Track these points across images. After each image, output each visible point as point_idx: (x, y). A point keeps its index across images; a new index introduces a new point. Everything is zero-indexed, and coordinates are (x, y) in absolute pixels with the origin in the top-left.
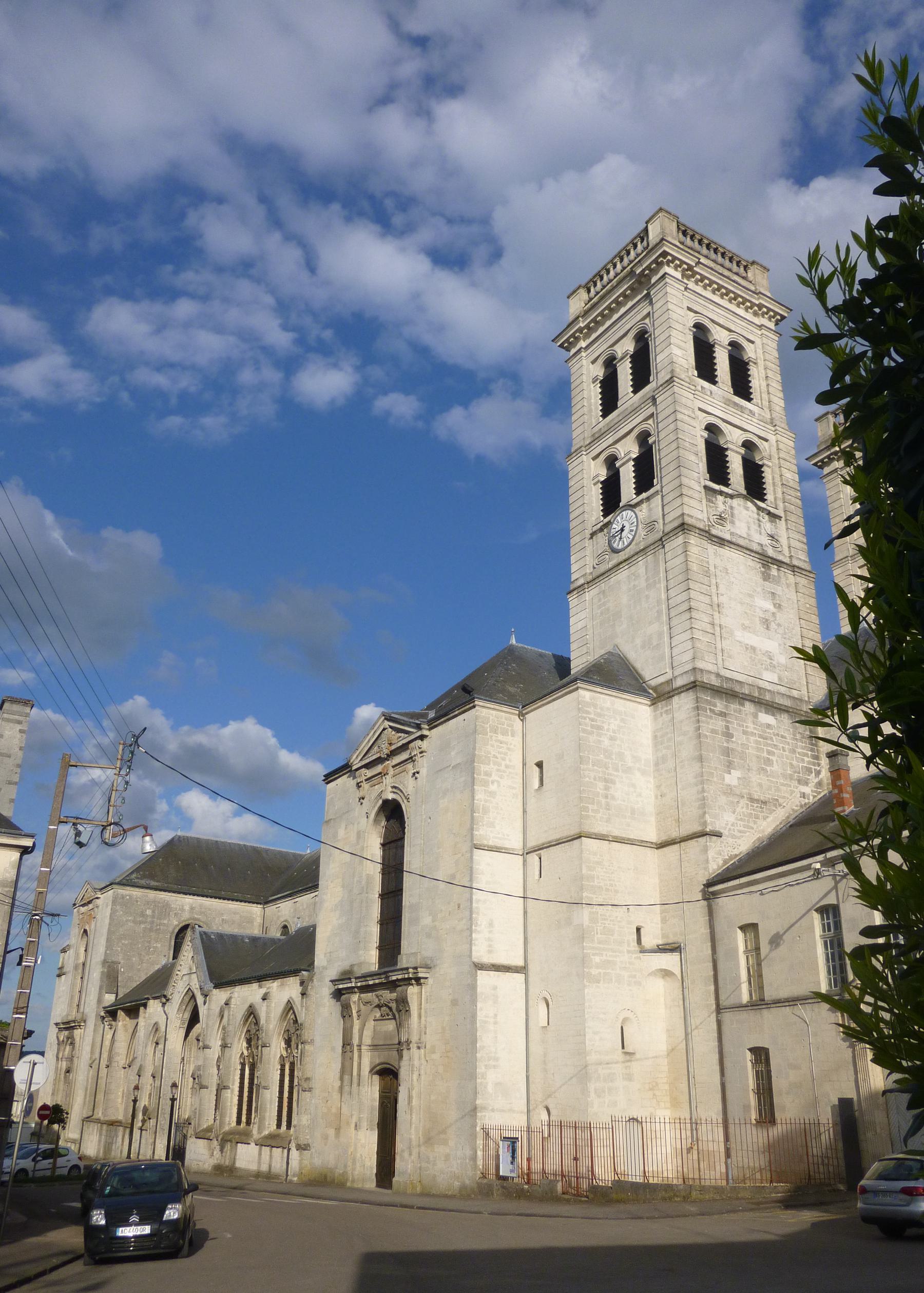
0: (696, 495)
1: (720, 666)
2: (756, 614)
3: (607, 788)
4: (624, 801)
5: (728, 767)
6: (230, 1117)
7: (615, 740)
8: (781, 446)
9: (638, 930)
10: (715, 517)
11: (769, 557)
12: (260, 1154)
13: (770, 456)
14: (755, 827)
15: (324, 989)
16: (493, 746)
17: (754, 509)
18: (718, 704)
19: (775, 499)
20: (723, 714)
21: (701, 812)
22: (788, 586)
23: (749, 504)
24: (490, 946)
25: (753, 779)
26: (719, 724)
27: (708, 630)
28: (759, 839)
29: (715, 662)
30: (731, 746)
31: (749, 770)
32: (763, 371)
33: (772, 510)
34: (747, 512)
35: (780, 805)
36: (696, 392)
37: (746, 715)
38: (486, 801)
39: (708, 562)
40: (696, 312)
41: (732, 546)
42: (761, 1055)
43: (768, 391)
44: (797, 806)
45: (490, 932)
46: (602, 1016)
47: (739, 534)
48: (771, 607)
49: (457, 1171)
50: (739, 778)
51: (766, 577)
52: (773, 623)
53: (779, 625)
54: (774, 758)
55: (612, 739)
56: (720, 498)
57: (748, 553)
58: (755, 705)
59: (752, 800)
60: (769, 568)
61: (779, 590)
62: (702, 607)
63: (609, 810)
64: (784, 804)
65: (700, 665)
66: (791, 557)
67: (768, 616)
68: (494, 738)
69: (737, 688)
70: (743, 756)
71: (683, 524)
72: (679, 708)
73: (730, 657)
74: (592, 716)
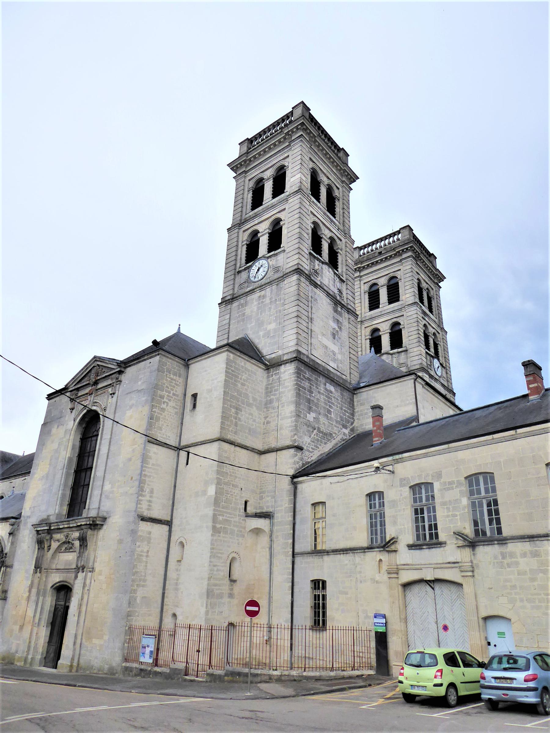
3: (237, 413)
4: (245, 423)
9: (246, 503)
16: (166, 380)
68: (168, 376)
74: (233, 369)
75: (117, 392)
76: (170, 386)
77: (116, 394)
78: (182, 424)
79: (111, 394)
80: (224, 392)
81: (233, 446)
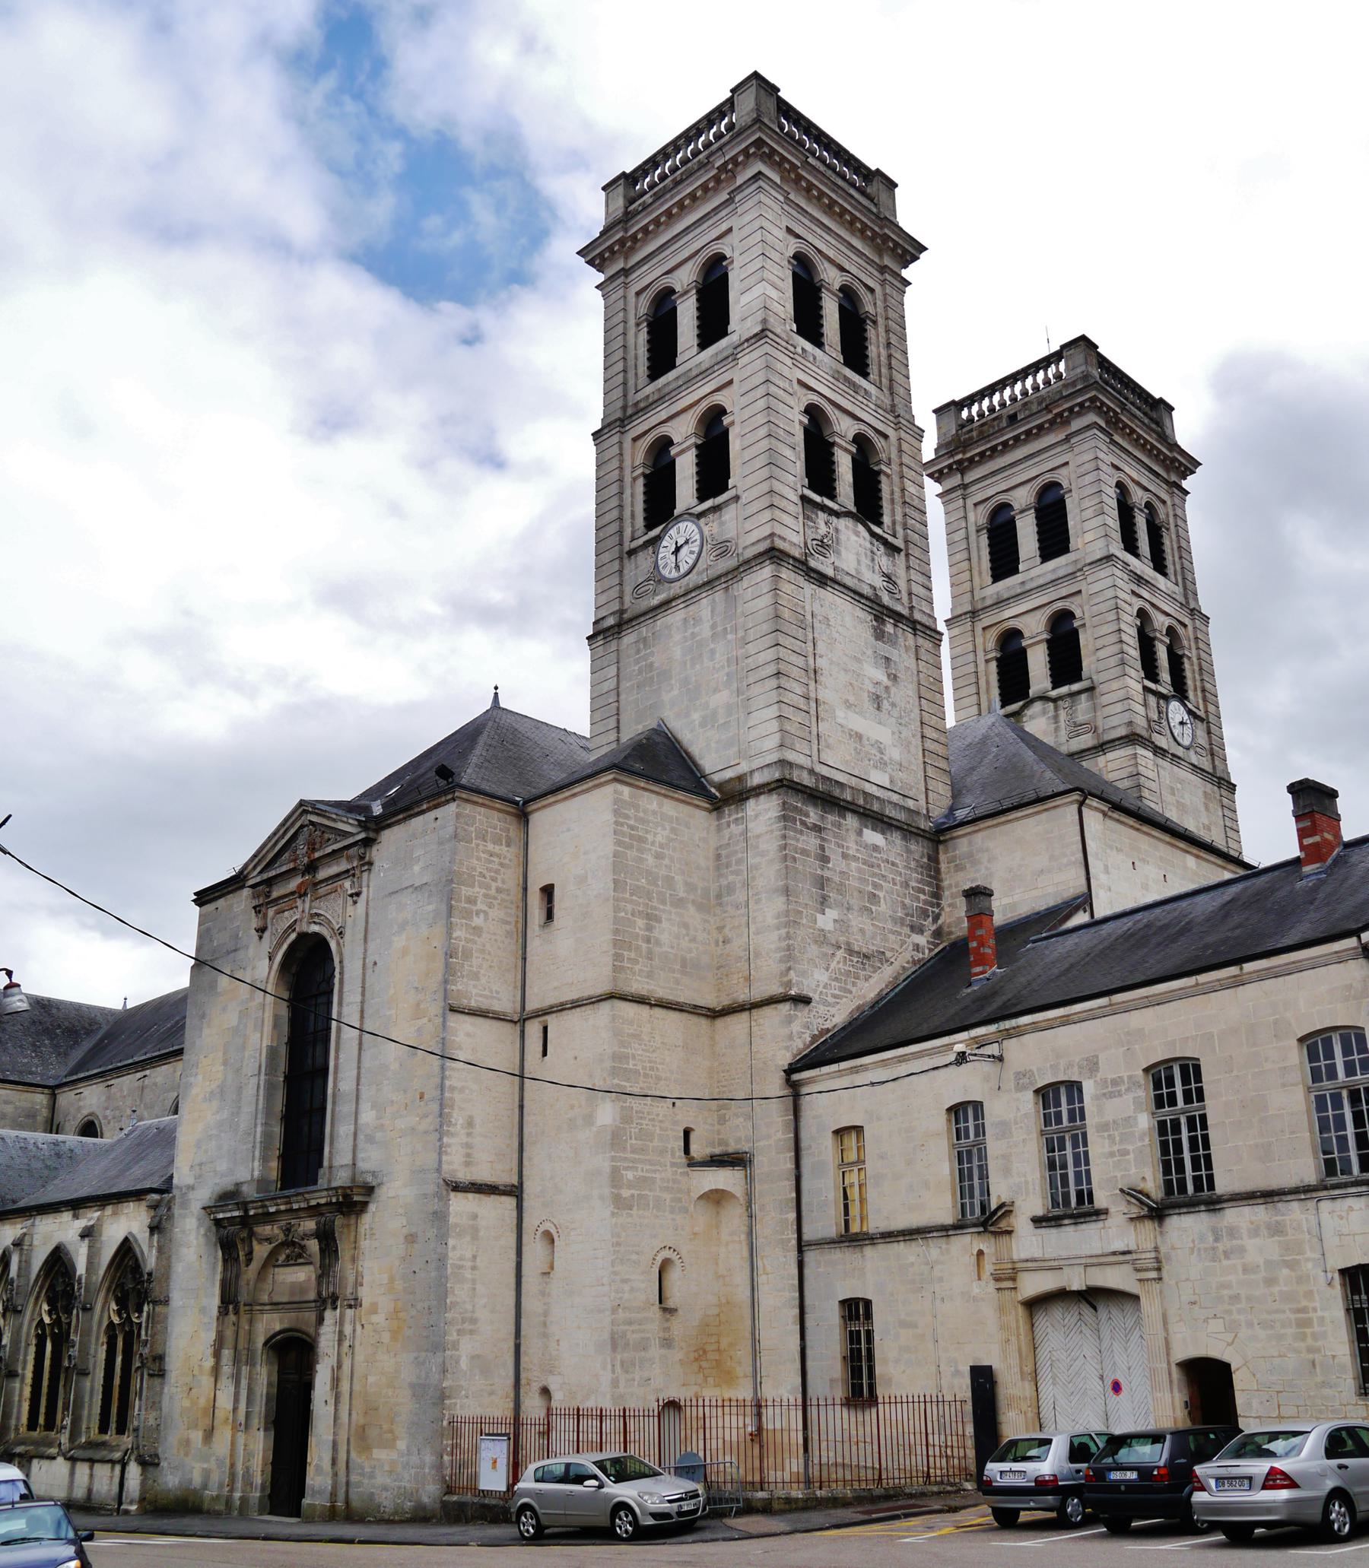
0: (791, 508)
1: (815, 758)
2: (865, 687)
3: (649, 928)
4: (672, 947)
5: (822, 903)
6: (18, 1418)
7: (663, 858)
8: (905, 447)
9: (687, 1133)
10: (815, 542)
11: (883, 606)
12: (72, 1473)
13: (890, 459)
14: (854, 990)
15: (188, 1220)
16: (479, 859)
17: (867, 535)
18: (812, 814)
19: (894, 523)
20: (817, 829)
21: (783, 967)
22: (907, 649)
23: (861, 528)
24: (468, 1155)
25: (853, 923)
26: (810, 841)
27: (801, 706)
28: (858, 1008)
29: (808, 753)
30: (827, 874)
31: (848, 909)
32: (884, 334)
33: (890, 539)
34: (856, 538)
35: (887, 961)
36: (796, 356)
37: (848, 830)
38: (467, 940)
39: (804, 607)
40: (798, 236)
41: (836, 587)
42: (856, 1310)
43: (890, 364)
44: (908, 962)
45: (469, 1134)
46: (634, 1257)
47: (846, 569)
48: (884, 679)
49: (408, 1485)
50: (835, 921)
51: (879, 635)
52: (885, 702)
53: (893, 705)
54: (881, 894)
55: (659, 856)
56: (822, 516)
57: (857, 598)
58: (860, 819)
59: (851, 952)
60: (883, 622)
61: (894, 654)
62: (795, 672)
63: (651, 959)
64: (892, 960)
65: (791, 756)
66: (911, 608)
67: (880, 691)
68: (481, 847)
69: (837, 792)
70: (841, 889)
71: (772, 549)
72: (757, 816)
73: (828, 746)
74: (631, 822)
75: (364, 890)
76: (489, 870)
77: (364, 896)
78: (524, 959)
79: (351, 896)
80: (615, 881)
81: (648, 1007)
